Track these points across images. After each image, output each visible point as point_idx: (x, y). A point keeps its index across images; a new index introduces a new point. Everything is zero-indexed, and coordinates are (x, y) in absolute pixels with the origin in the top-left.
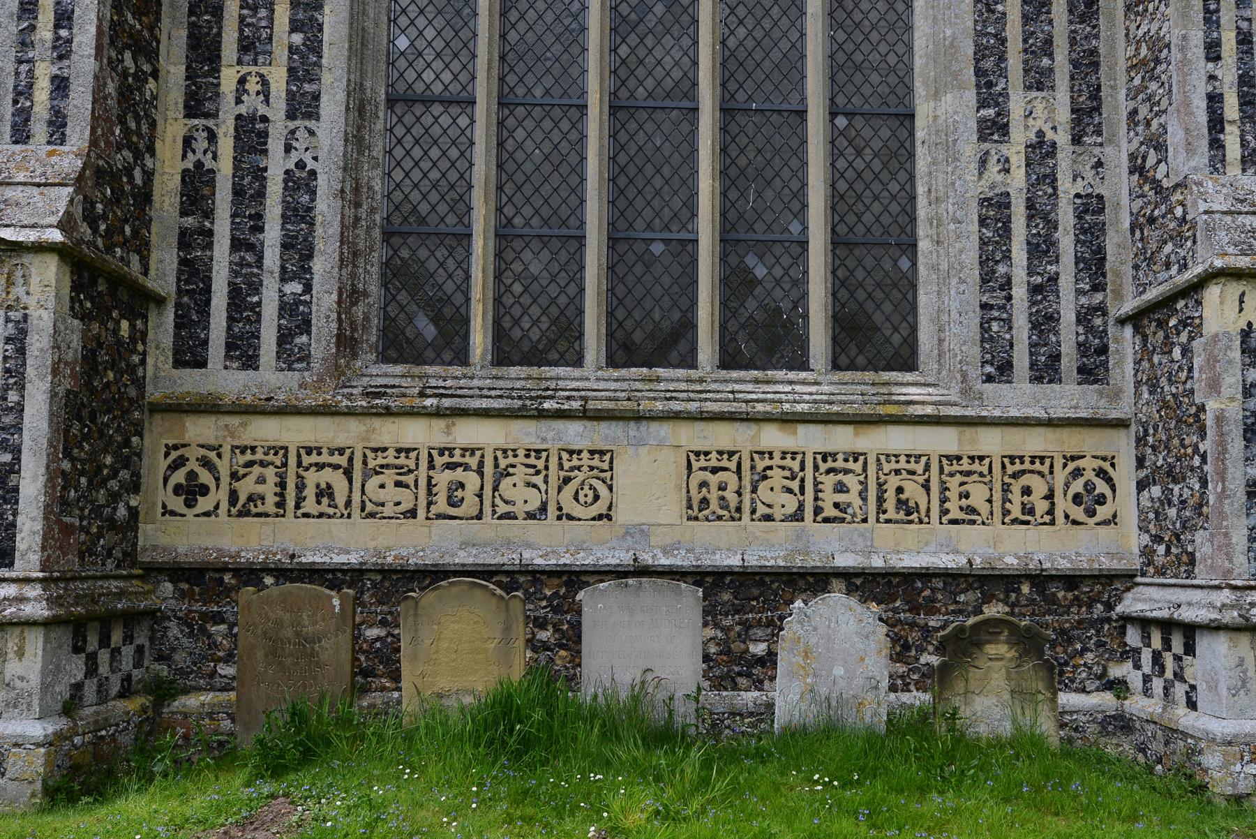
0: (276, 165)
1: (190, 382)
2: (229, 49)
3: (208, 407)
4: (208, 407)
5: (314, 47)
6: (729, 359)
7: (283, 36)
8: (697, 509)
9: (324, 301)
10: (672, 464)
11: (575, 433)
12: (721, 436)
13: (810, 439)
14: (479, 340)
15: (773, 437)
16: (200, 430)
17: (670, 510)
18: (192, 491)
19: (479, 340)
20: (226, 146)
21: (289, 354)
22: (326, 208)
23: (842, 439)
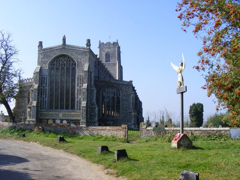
0: (44, 100)
1: (41, 110)
2: (42, 94)
3: (42, 111)
4: (42, 111)
5: (46, 94)
6: (60, 109)
7: (45, 94)
8: (63, 116)
9: (47, 106)
10: (62, 114)
11: (58, 113)
12: (64, 113)
13: (68, 113)
14: (54, 108)
15: (66, 113)
16: (41, 113)
17: (62, 117)
18: (41, 115)
19: (54, 108)
20: (42, 99)
21: (45, 109)
22: (47, 102)
23: (70, 113)
